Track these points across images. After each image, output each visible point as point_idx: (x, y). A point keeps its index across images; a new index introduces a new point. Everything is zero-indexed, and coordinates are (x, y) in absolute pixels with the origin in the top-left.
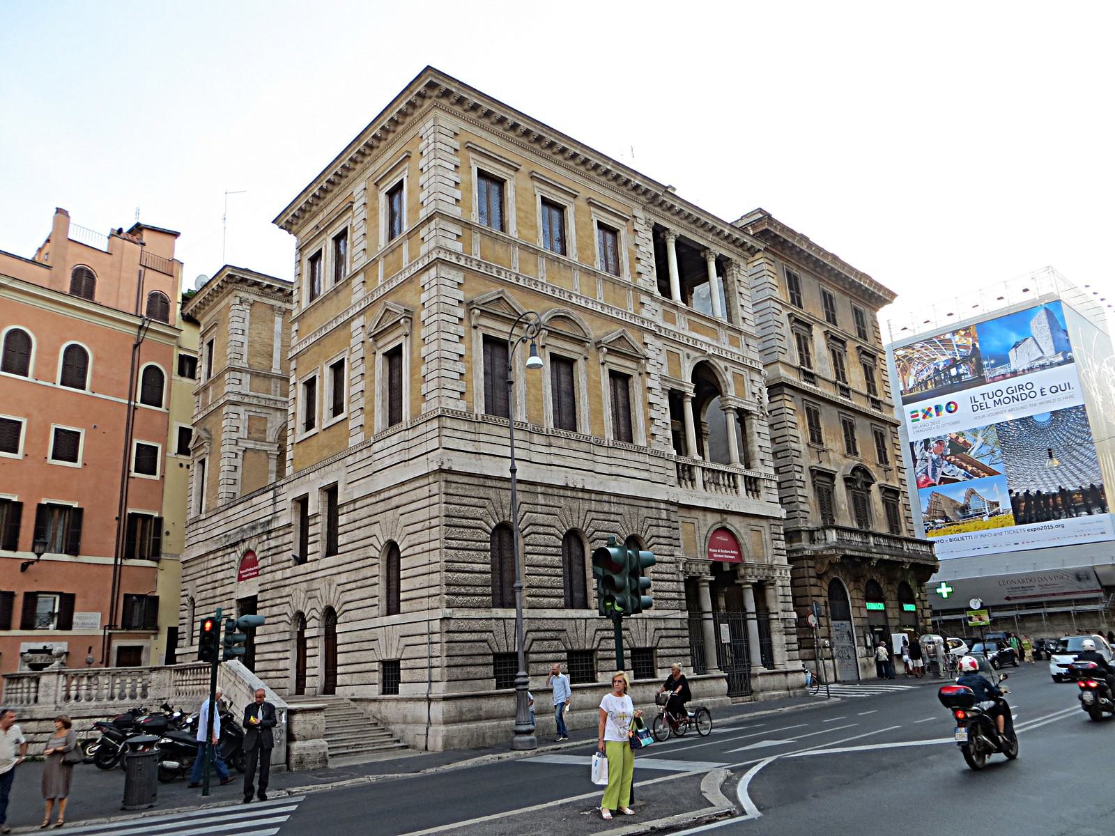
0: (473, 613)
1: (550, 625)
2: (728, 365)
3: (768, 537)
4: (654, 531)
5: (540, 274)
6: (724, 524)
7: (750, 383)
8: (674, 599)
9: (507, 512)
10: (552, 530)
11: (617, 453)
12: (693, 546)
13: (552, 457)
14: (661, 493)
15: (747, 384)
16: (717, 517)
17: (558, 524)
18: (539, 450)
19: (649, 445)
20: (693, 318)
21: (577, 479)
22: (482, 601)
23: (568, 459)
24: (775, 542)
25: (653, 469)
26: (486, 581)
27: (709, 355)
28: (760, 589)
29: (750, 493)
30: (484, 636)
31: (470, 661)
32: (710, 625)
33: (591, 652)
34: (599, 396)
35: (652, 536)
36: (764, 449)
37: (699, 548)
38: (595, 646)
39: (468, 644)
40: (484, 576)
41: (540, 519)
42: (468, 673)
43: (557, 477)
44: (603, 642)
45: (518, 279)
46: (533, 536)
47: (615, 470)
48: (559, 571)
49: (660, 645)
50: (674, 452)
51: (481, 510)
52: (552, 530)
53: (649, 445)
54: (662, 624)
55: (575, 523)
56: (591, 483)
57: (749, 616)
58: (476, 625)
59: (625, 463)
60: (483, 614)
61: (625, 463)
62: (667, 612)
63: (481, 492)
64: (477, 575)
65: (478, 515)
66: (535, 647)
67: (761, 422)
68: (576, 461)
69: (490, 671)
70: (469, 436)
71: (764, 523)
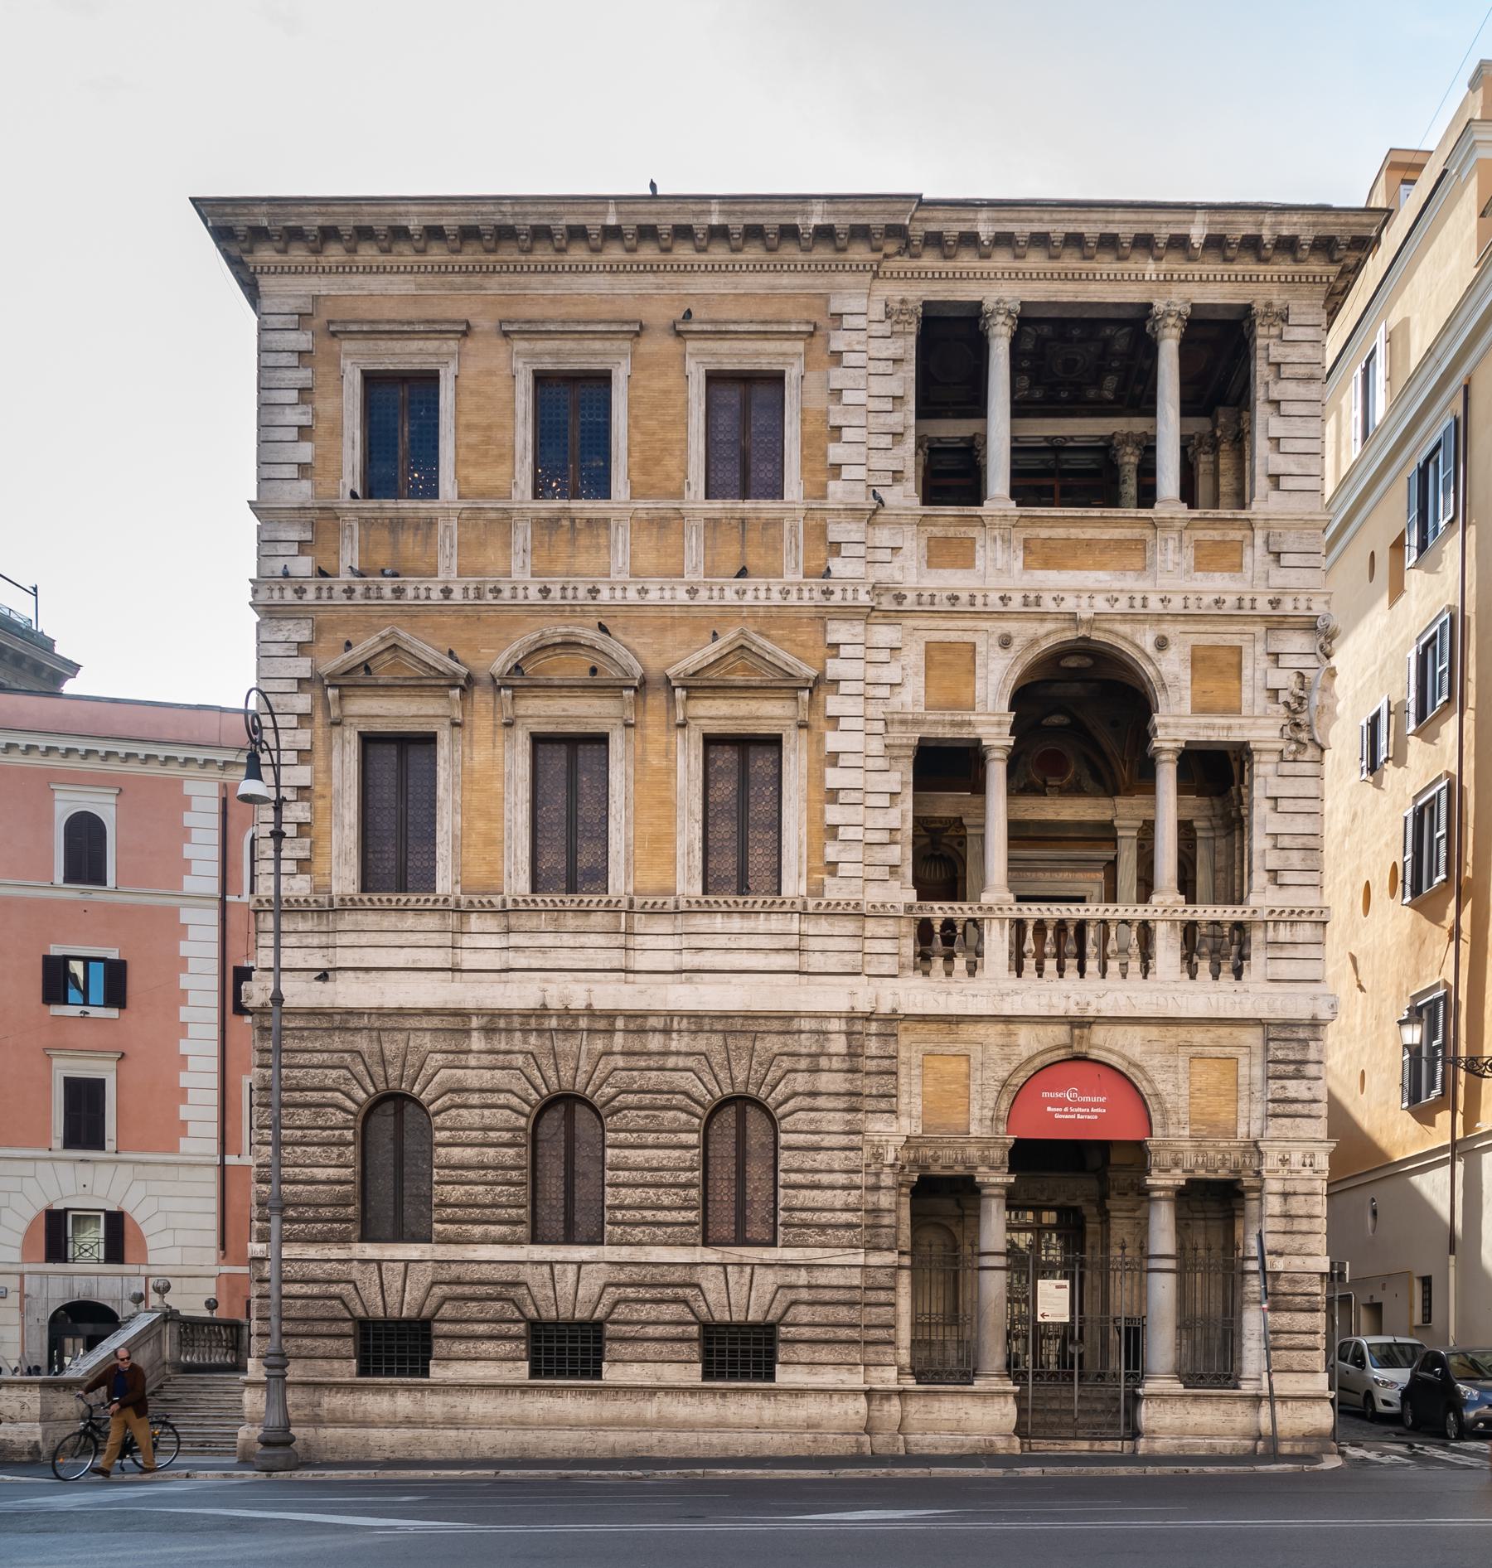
0: (312, 1252)
1: (487, 1272)
2: (1168, 629)
3: (1258, 1072)
4: (801, 1082)
5: (516, 564)
6: (1076, 1049)
7: (1265, 662)
8: (849, 1226)
9: (393, 1072)
10: (502, 1099)
11: (701, 922)
12: (962, 1107)
13: (511, 954)
14: (832, 997)
15: (1255, 668)
16: (1060, 1034)
17: (520, 1085)
18: (483, 942)
19: (817, 891)
20: (1044, 533)
21: (575, 993)
22: (331, 1230)
23: (553, 954)
24: (1274, 1085)
25: (813, 944)
26: (346, 1195)
27: (1090, 623)
28: (1217, 1201)
29: (1204, 965)
30: (334, 1289)
31: (302, 1329)
32: (994, 1285)
33: (598, 1325)
34: (669, 805)
35: (795, 1094)
36: (1285, 842)
37: (975, 1110)
38: (598, 1314)
39: (299, 1302)
40: (338, 1188)
41: (472, 1078)
42: (298, 1347)
43: (519, 994)
44: (621, 1308)
45: (447, 592)
46: (453, 1112)
47: (689, 960)
48: (514, 1175)
49: (789, 1318)
50: (911, 896)
51: (334, 1073)
52: (502, 1099)
53: (817, 891)
54: (802, 1277)
55: (567, 1077)
56: (611, 994)
57: (1170, 1264)
58: (317, 1271)
59: (722, 941)
60: (335, 1252)
61: (722, 941)
62: (819, 1252)
63: (337, 1041)
64: (321, 1187)
65: (329, 1082)
66: (447, 1310)
67: (1287, 768)
68: (576, 954)
69: (348, 1346)
70: (315, 940)
71: (1252, 1037)
